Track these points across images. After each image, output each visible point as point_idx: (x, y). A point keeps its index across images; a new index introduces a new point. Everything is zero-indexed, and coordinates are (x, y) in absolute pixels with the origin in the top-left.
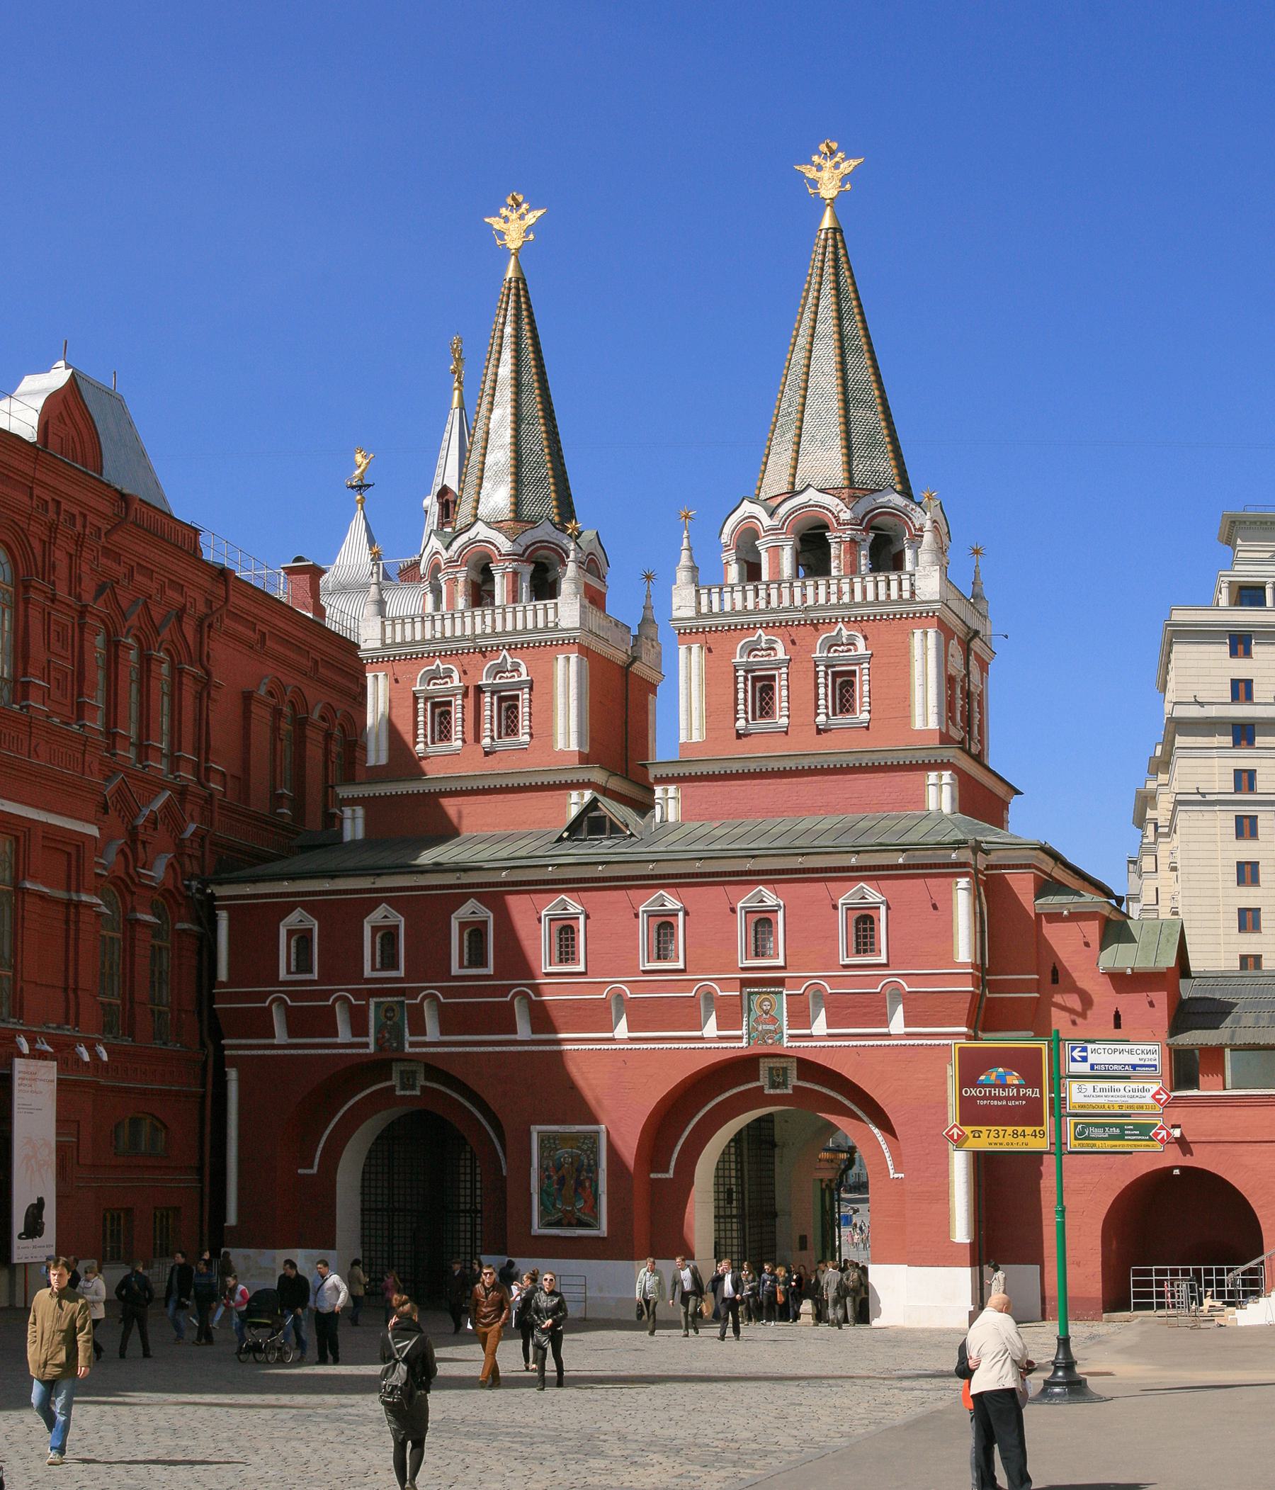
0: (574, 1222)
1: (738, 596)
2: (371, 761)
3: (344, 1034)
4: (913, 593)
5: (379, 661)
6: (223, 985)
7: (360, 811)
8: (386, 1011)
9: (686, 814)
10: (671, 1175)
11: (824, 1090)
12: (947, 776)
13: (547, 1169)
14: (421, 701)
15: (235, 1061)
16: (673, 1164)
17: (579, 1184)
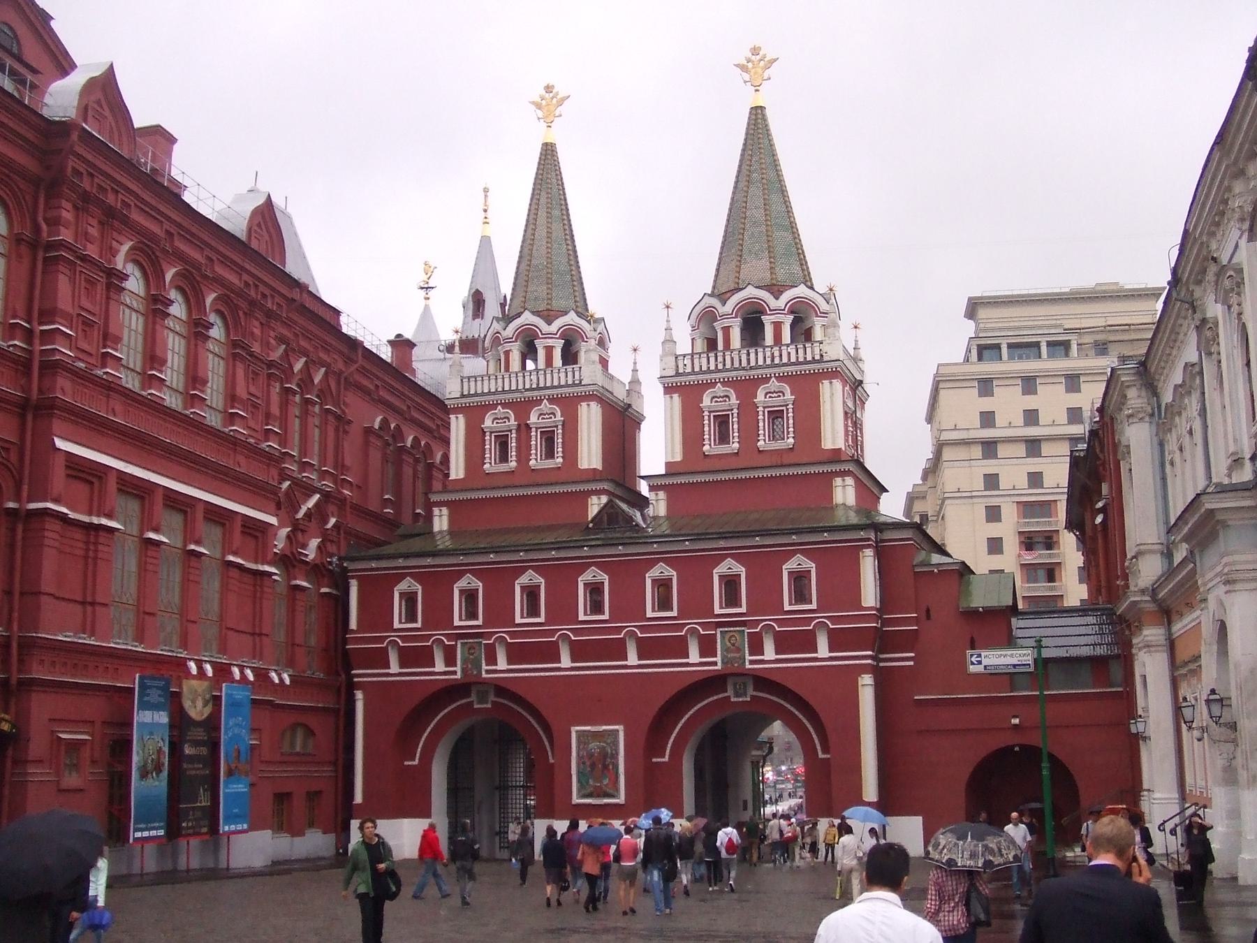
1: (704, 361)
2: (453, 476)
3: (440, 666)
5: (457, 410)
7: (445, 511)
10: (666, 759)
12: (850, 481)
15: (360, 686)
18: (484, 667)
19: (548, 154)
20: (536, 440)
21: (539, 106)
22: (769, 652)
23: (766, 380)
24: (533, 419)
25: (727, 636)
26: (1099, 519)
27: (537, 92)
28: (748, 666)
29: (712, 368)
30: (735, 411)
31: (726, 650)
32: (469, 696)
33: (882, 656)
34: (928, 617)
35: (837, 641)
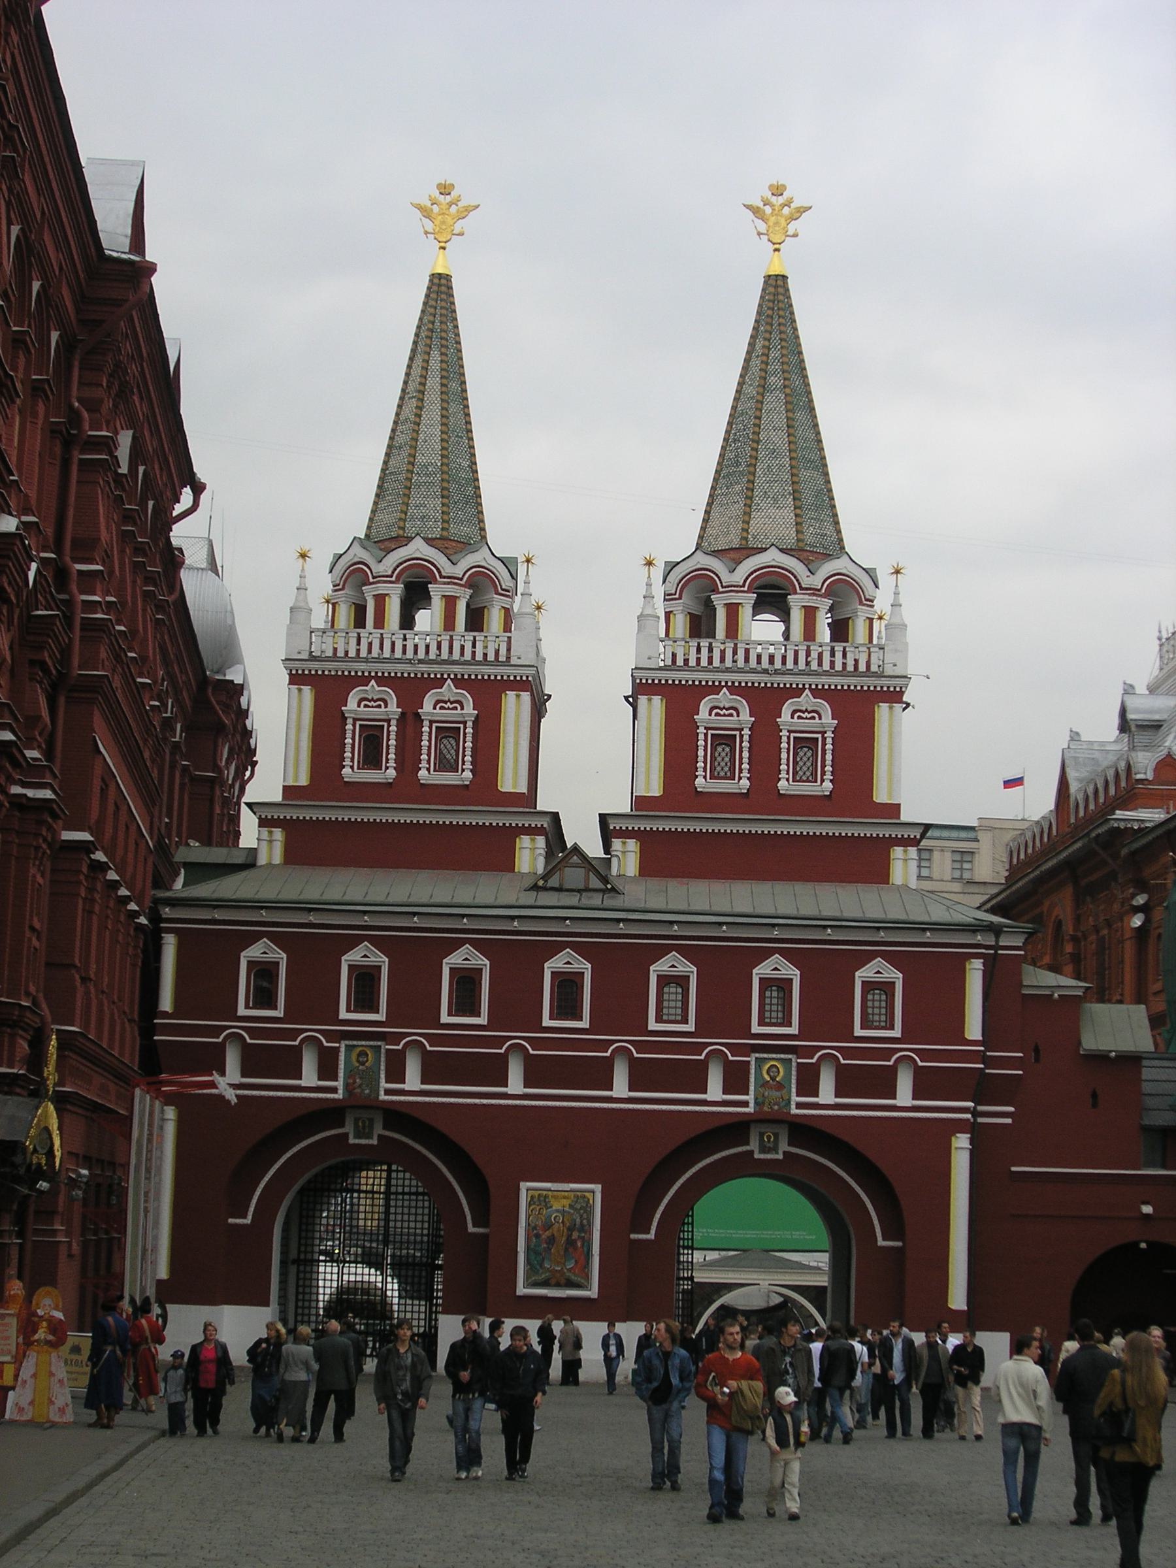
0: (563, 1281)
3: (309, 1076)
6: (165, 1015)
8: (359, 1055)
9: (646, 869)
10: (651, 1236)
13: (535, 1228)
14: (350, 721)
17: (571, 1243)
18: (384, 1085)
19: (440, 289)
21: (426, 213)
22: (827, 1093)
23: (797, 692)
26: (1137, 921)
27: (426, 192)
28: (794, 1111)
30: (746, 732)
32: (342, 1125)
33: (980, 1108)
35: (924, 1086)
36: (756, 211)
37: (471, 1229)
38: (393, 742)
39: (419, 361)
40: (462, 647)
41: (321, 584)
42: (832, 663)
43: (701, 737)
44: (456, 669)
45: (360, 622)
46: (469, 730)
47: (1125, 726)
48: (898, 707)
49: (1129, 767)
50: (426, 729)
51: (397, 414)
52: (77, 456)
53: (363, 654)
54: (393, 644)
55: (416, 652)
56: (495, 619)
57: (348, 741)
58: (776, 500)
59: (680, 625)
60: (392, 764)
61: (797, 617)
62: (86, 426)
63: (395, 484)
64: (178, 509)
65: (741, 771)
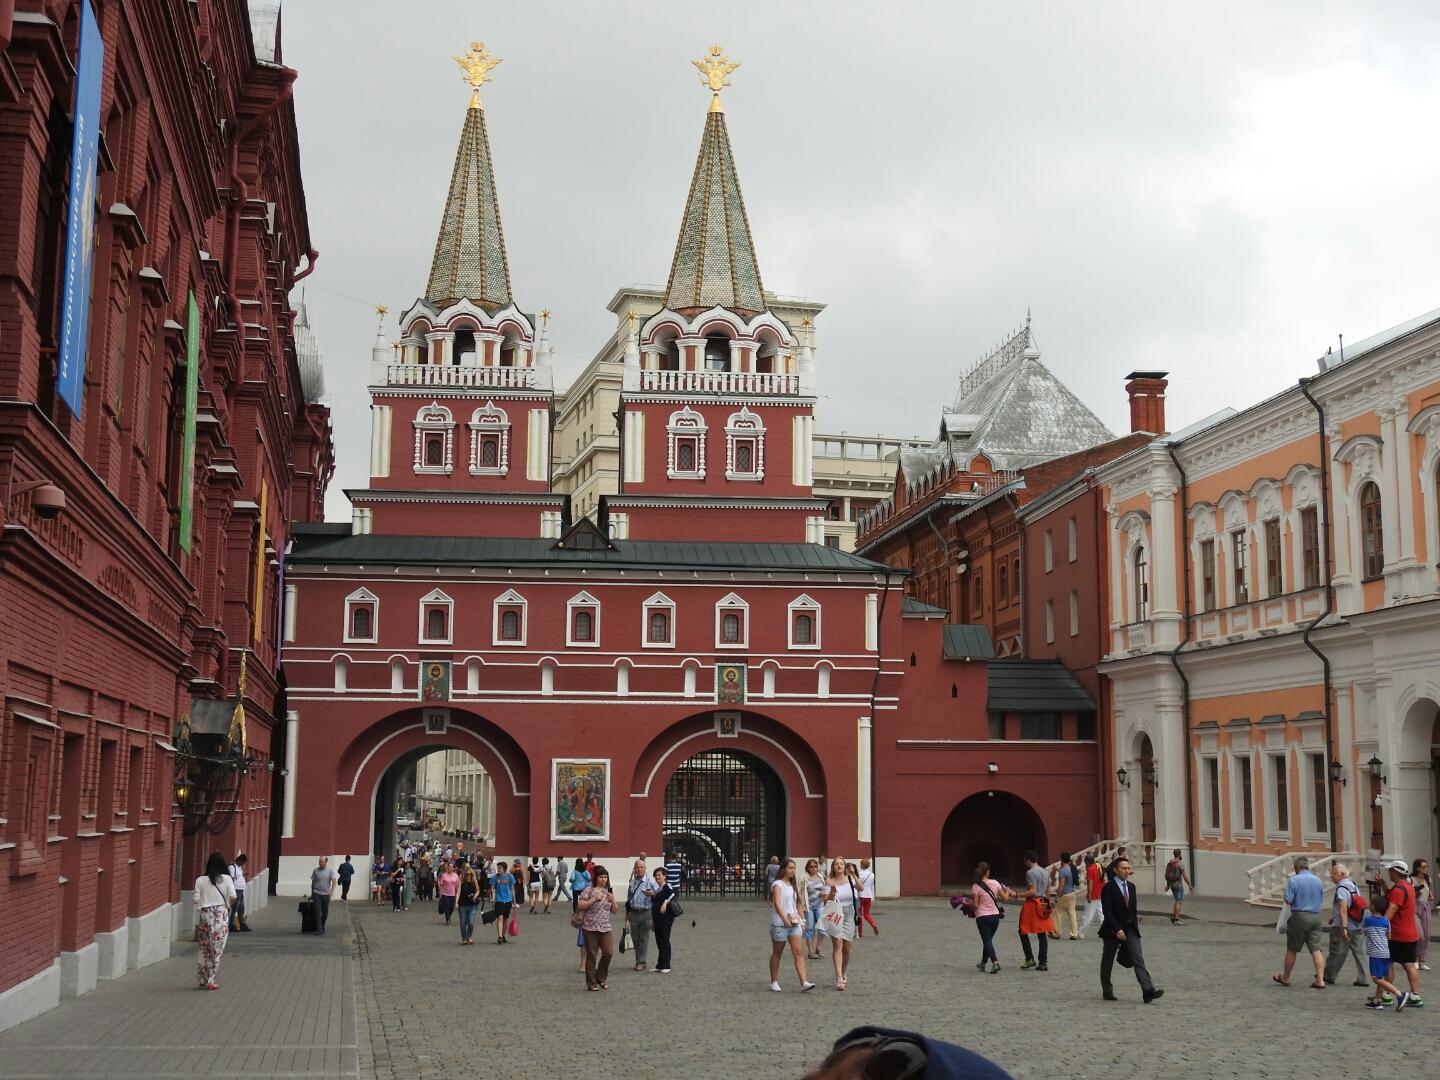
3: (397, 686)
4: (797, 388)
6: (290, 644)
10: (646, 795)
11: (760, 736)
14: (418, 431)
15: (297, 705)
16: (648, 786)
17: (589, 802)
18: (452, 691)
20: (475, 444)
22: (769, 690)
23: (738, 408)
24: (475, 420)
25: (726, 672)
26: (961, 569)
28: (746, 703)
29: (664, 388)
30: (703, 437)
31: (723, 685)
34: (913, 664)
36: (700, 67)
37: (516, 794)
38: (450, 446)
39: (461, 171)
40: (499, 378)
41: (394, 332)
42: (763, 388)
43: (671, 440)
44: (496, 392)
45: (423, 359)
46: (505, 437)
47: (944, 434)
48: (809, 418)
49: (952, 463)
50: (474, 436)
51: (446, 210)
52: (239, 217)
53: (428, 382)
54: (449, 375)
55: (465, 381)
56: (520, 357)
57: (418, 445)
58: (719, 273)
59: (653, 361)
60: (449, 461)
61: (736, 356)
62: (246, 194)
63: (445, 259)
64: (298, 271)
65: (699, 464)
